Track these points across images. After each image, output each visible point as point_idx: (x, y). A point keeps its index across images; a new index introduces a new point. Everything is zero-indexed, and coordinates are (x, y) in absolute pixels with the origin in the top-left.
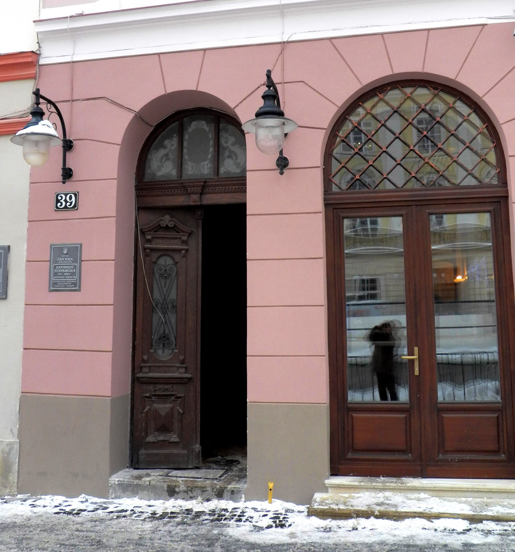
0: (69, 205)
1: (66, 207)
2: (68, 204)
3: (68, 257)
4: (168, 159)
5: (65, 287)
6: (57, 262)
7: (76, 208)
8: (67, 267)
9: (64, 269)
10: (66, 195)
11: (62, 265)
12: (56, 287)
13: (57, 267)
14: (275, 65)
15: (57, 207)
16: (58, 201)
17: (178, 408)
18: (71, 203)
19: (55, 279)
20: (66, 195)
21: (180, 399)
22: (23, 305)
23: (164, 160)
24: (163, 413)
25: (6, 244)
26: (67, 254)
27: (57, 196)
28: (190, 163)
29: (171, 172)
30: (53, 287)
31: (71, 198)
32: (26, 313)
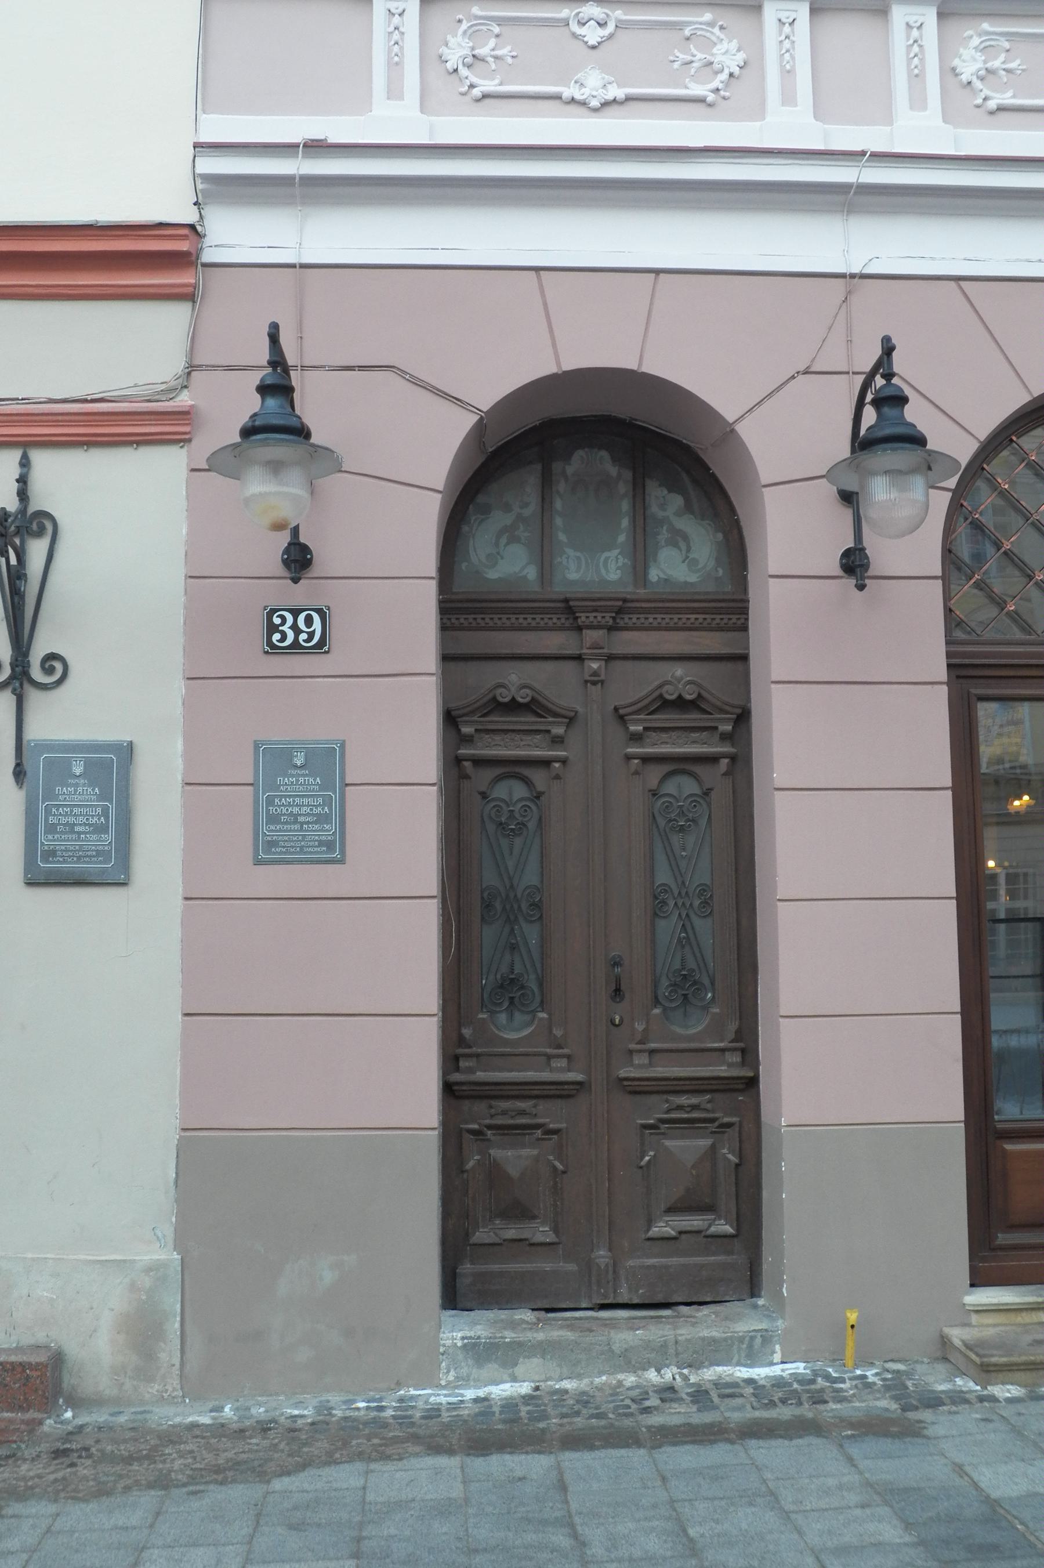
0: (304, 641)
1: (296, 644)
2: (303, 637)
3: (306, 775)
4: (514, 539)
5: (302, 852)
6: (277, 788)
7: (326, 648)
8: (306, 801)
9: (297, 805)
10: (295, 613)
11: (290, 796)
12: (274, 853)
13: (276, 800)
14: (830, 328)
15: (273, 646)
16: (272, 628)
17: (551, 1158)
18: (311, 635)
19: (272, 831)
20: (295, 613)
21: (555, 1137)
22: (179, 901)
23: (503, 540)
24: (514, 1172)
25: (122, 736)
26: (302, 767)
27: (270, 615)
28: (570, 552)
29: (524, 573)
30: (267, 851)
31: (309, 621)
32: (186, 923)
